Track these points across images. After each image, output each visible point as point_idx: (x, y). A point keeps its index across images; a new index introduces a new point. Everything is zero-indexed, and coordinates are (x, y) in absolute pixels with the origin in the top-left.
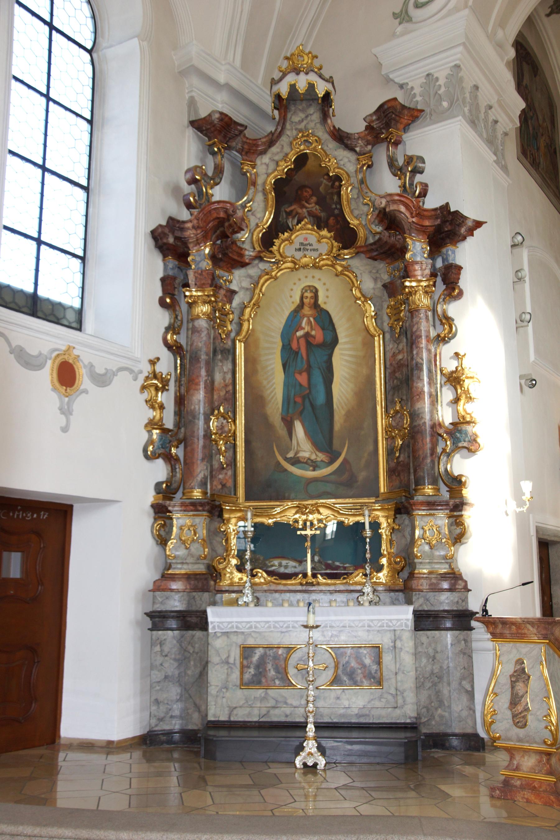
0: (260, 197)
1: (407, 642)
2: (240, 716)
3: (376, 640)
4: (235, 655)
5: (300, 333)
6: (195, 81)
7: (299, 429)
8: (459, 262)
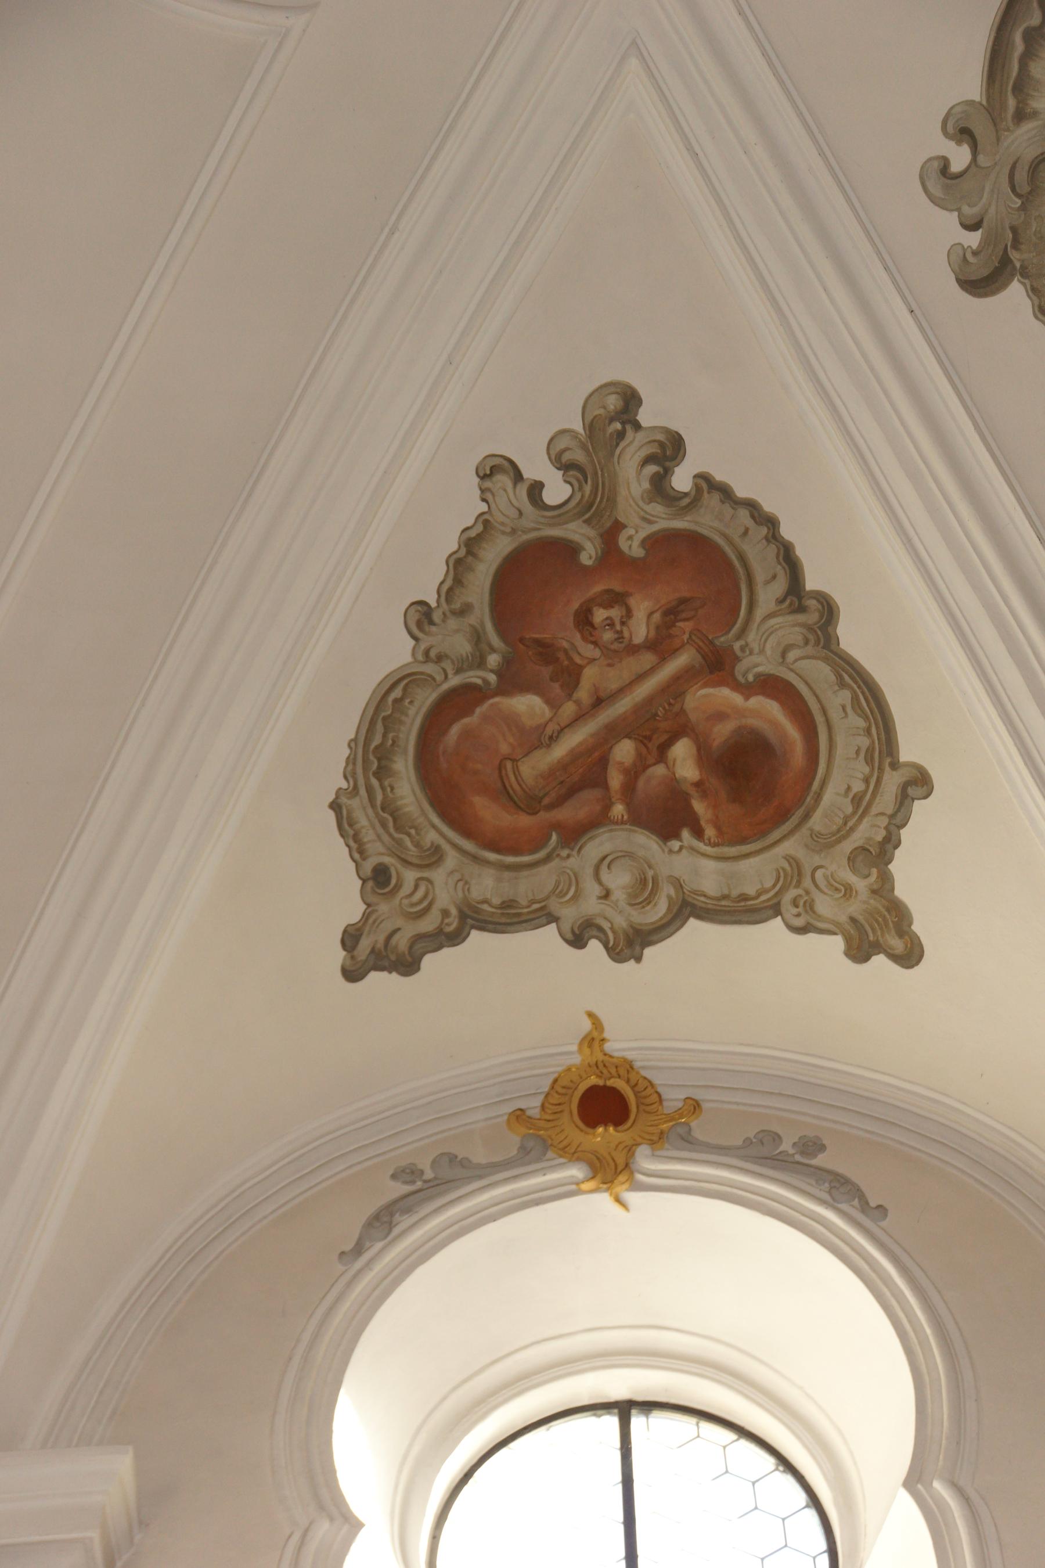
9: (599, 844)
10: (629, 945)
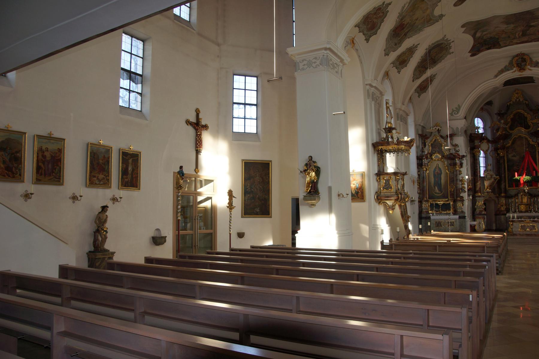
1: (458, 221)
4: (434, 223)
7: (436, 188)
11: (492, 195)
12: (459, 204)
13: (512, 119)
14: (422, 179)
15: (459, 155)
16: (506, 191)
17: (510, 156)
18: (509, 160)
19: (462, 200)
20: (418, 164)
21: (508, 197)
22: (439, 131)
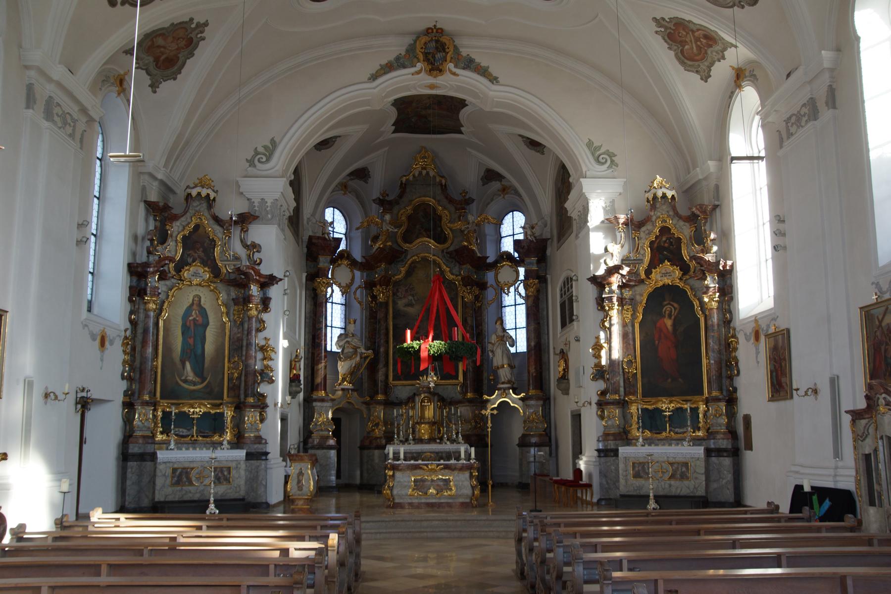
0: (172, 244)
1: (243, 466)
2: (170, 498)
3: (230, 465)
4: (169, 471)
5: (191, 318)
6: (146, 177)
7: (188, 366)
8: (270, 296)
9: (709, 52)
10: (723, 58)
11: (355, 398)
12: (251, 417)
13: (409, 218)
14: (140, 337)
15: (258, 273)
16: (387, 389)
17: (401, 304)
18: (397, 314)
19: (261, 404)
20: (131, 288)
21: (389, 404)
22: (210, 202)
